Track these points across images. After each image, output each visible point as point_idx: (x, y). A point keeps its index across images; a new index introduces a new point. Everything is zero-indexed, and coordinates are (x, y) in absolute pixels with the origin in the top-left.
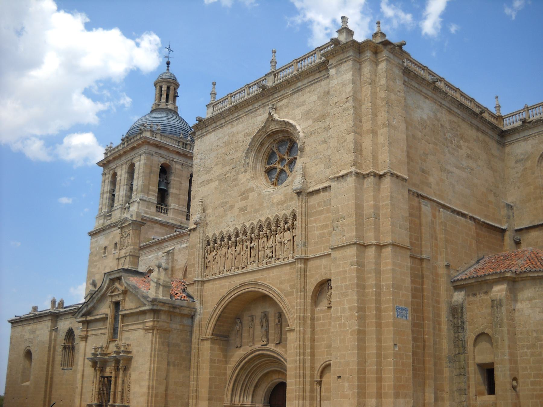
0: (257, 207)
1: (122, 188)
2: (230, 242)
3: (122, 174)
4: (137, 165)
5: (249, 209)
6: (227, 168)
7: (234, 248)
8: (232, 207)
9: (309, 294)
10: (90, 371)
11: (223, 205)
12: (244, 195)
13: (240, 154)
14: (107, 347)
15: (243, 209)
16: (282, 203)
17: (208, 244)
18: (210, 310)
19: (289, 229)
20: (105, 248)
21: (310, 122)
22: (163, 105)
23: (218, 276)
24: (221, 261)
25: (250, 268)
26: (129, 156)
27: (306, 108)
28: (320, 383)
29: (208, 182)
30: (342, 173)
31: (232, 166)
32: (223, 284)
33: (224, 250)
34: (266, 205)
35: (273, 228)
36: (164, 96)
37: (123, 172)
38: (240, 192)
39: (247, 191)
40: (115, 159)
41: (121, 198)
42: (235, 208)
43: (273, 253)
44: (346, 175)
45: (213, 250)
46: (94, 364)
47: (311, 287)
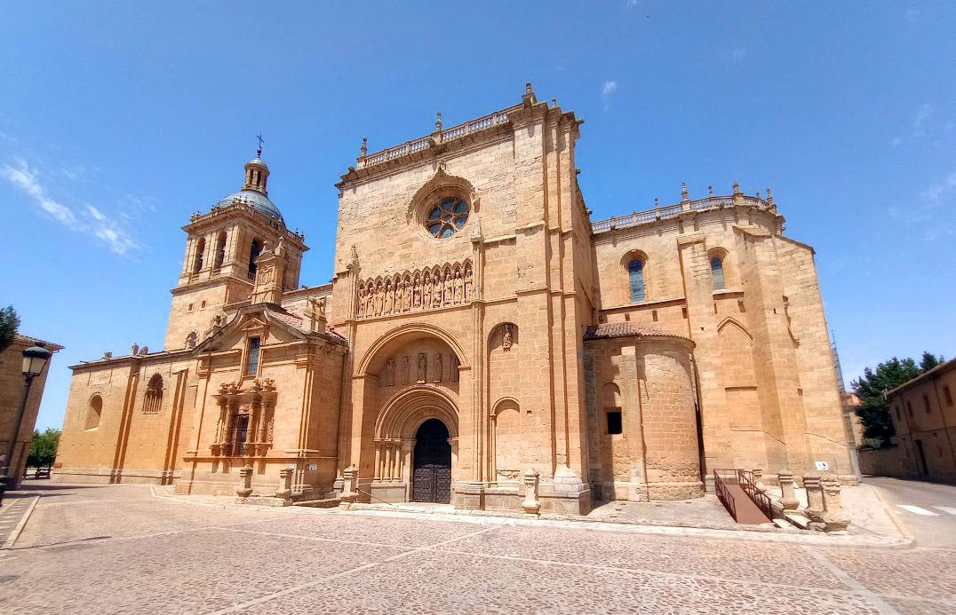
0: (422, 254)
1: (211, 253)
2: (389, 286)
3: (211, 241)
4: (229, 234)
5: (412, 257)
6: (386, 218)
7: (393, 292)
8: (391, 254)
9: (486, 336)
10: (214, 411)
11: (379, 252)
12: (407, 243)
13: (403, 206)
14: (240, 384)
15: (403, 257)
16: (454, 252)
17: (362, 287)
18: (366, 349)
19: (460, 277)
20: (191, 305)
21: (487, 180)
22: (254, 188)
23: (374, 317)
24: (378, 304)
25: (413, 310)
26: (221, 225)
27: (480, 167)
28: (495, 418)
29: (361, 230)
30: (529, 226)
31: (391, 217)
33: (381, 294)
35: (442, 274)
36: (255, 179)
37: (213, 239)
39: (411, 240)
40: (203, 226)
41: (210, 262)
44: (536, 227)
46: (222, 402)
47: (488, 329)
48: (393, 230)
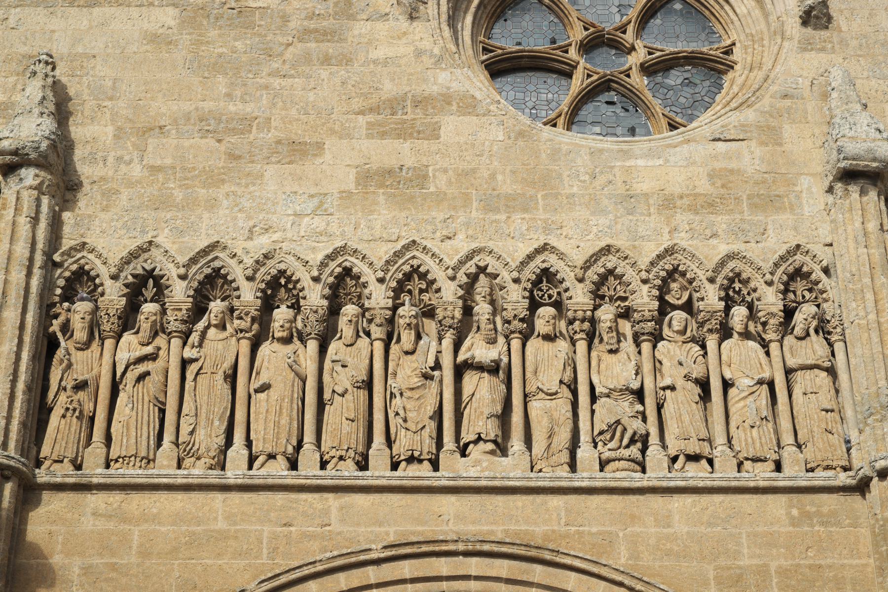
0: (507, 186)
5: (438, 183)
32: (221, 525)
34: (575, 190)
38: (365, 96)
42: (328, 156)
43: (644, 420)
45: (115, 327)
48: (305, 34)
